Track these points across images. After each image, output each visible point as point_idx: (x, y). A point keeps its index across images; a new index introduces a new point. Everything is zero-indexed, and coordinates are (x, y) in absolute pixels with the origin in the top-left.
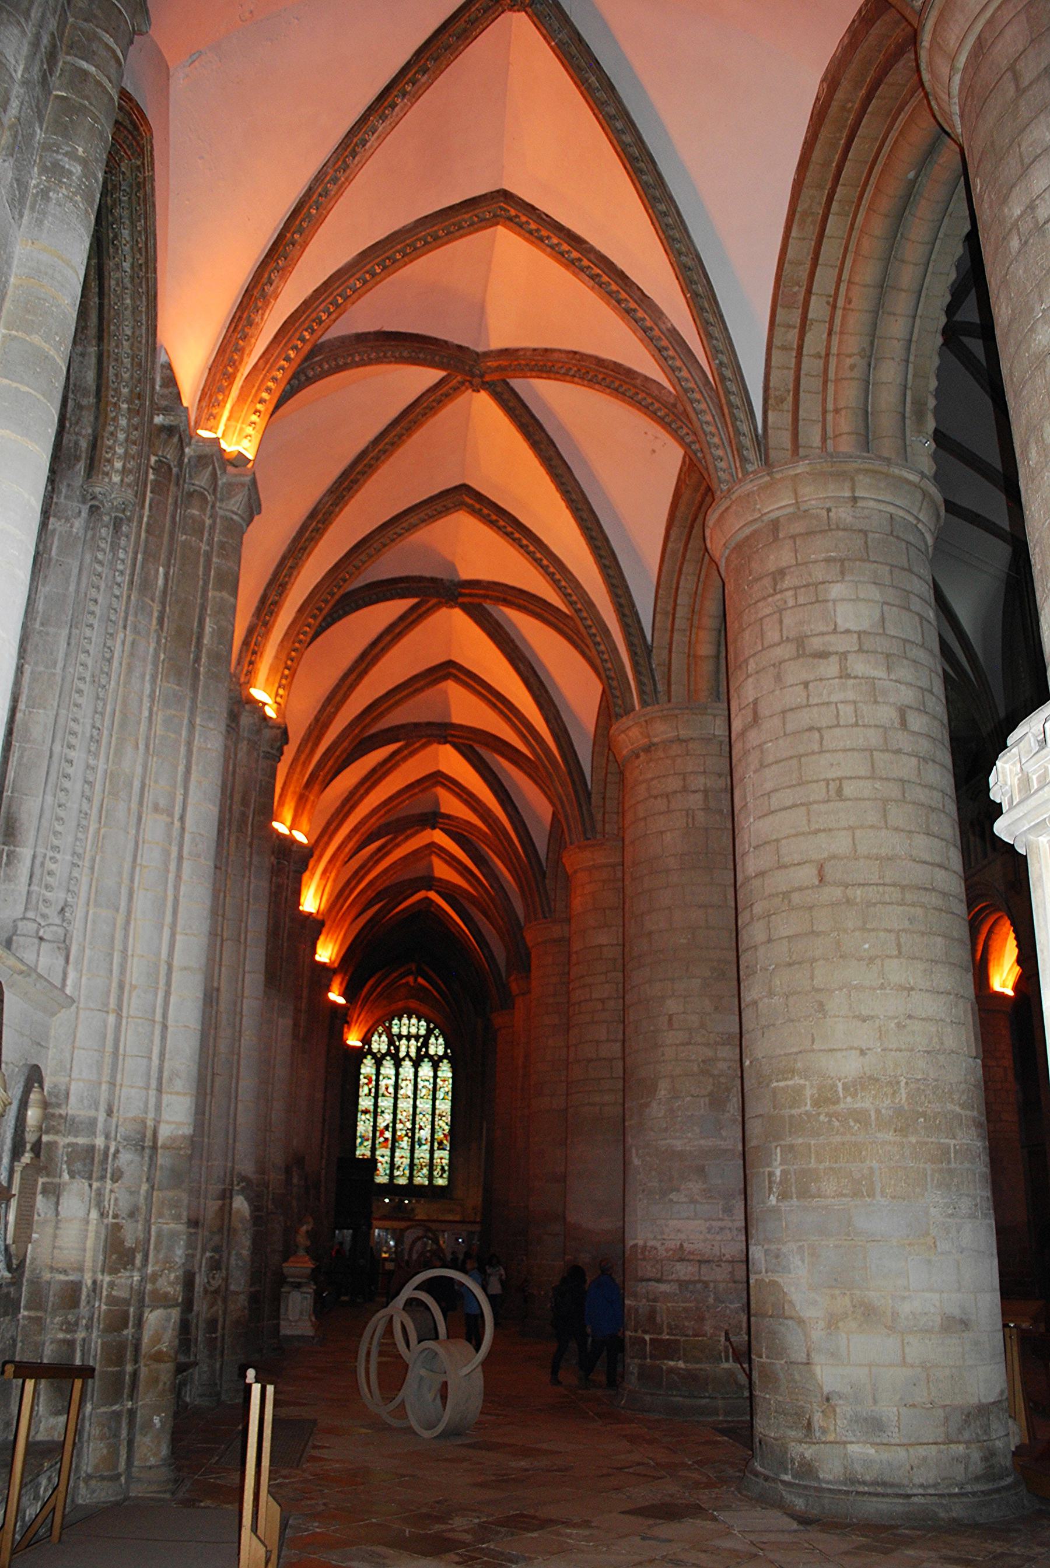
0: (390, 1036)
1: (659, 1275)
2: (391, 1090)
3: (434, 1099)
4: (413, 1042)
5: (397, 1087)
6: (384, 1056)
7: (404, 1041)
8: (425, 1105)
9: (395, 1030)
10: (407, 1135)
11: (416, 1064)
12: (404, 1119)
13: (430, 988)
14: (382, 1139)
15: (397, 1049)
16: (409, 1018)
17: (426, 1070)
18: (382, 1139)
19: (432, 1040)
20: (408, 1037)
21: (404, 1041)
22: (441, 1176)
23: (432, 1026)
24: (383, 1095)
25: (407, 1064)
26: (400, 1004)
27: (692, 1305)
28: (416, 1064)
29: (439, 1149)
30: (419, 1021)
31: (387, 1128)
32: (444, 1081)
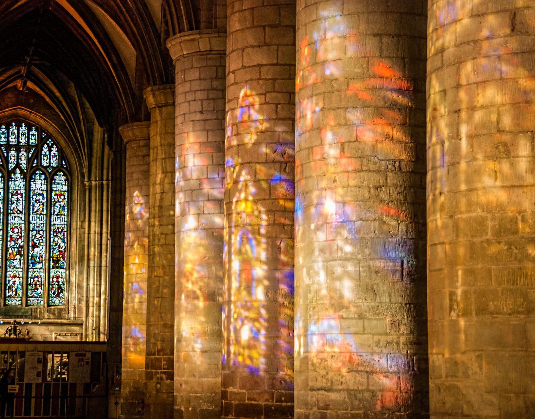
1: (329, 384)
3: (49, 215)
4: (23, 153)
7: (13, 153)
8: (38, 221)
10: (19, 253)
11: (28, 178)
13: (41, 92)
16: (18, 127)
19: (45, 151)
20: (18, 148)
21: (13, 153)
25: (17, 176)
26: (8, 111)
27: (361, 412)
28: (28, 178)
29: (53, 267)
30: (29, 130)
32: (60, 195)
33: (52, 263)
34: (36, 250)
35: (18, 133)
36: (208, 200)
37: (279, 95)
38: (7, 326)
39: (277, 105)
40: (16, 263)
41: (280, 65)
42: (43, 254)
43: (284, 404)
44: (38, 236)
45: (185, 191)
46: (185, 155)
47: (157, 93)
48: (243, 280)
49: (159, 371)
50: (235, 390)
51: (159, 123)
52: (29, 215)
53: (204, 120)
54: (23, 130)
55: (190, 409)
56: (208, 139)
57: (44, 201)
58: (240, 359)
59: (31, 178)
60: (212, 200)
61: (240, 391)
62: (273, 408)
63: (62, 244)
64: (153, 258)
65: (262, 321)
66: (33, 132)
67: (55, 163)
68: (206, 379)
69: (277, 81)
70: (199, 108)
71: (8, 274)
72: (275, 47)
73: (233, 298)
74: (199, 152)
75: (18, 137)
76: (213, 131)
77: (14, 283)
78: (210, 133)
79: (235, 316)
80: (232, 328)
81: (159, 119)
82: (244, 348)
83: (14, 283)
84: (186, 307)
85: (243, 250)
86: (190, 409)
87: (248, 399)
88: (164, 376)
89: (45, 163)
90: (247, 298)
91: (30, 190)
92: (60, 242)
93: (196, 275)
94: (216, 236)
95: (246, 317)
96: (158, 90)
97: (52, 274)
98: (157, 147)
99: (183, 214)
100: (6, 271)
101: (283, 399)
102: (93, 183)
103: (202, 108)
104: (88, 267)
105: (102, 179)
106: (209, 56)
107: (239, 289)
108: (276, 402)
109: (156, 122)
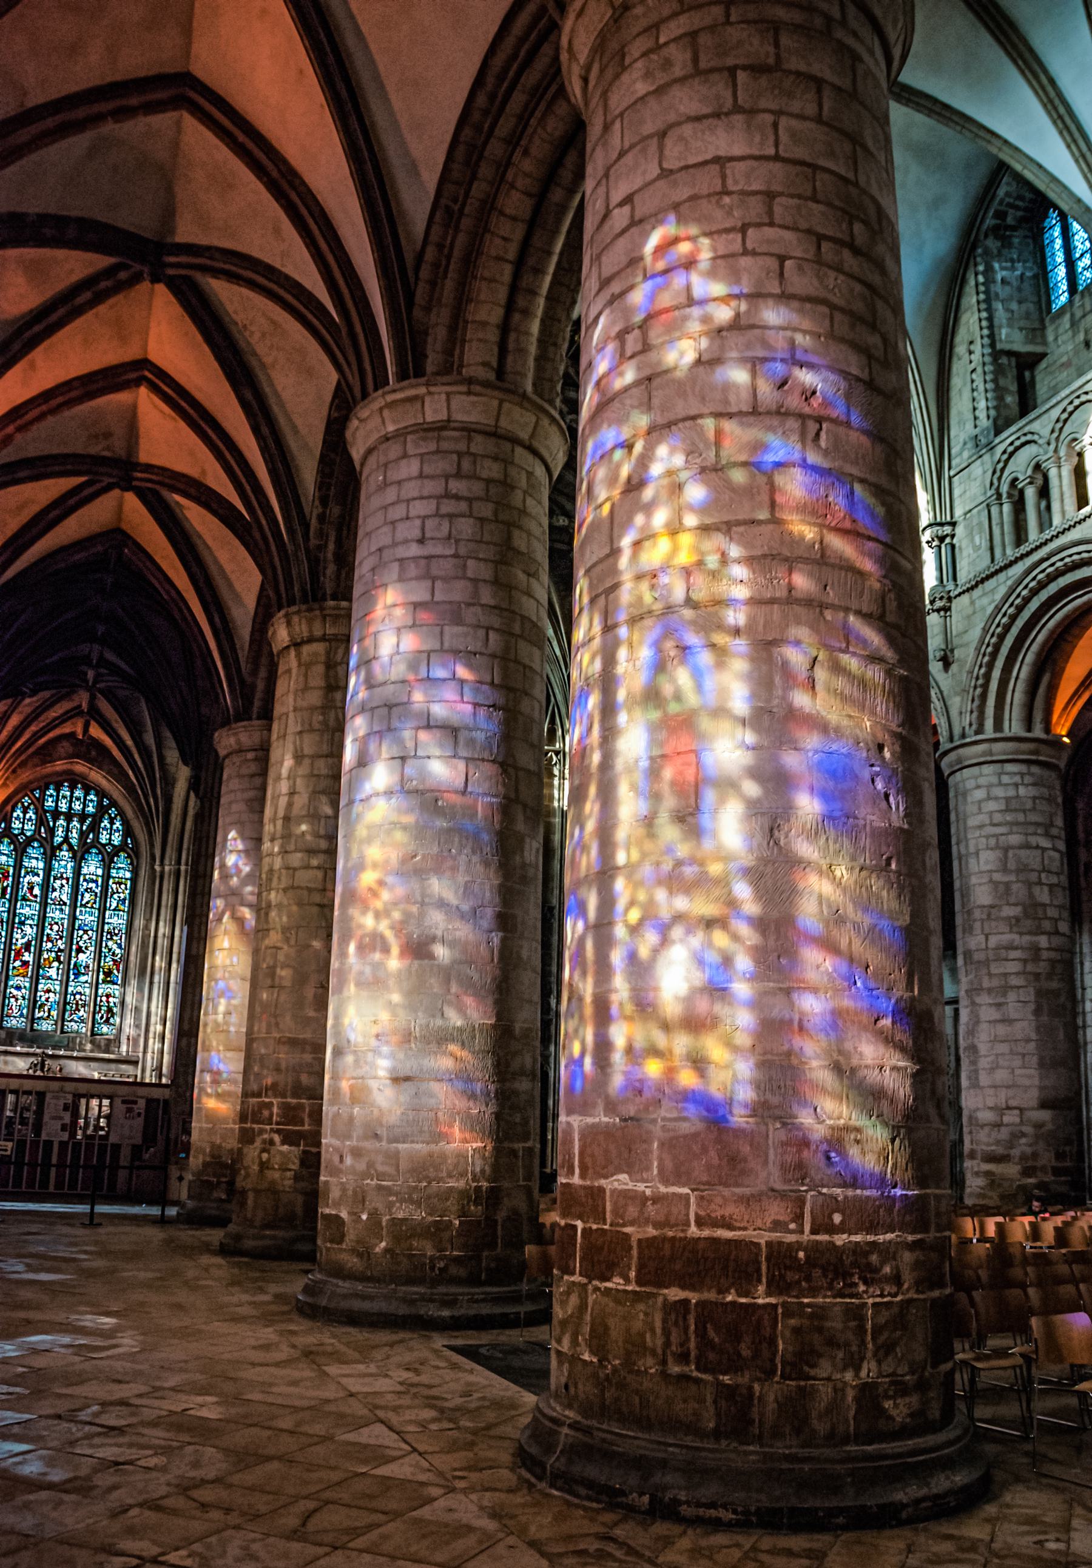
0: (41, 812)
2: (37, 891)
3: (103, 910)
4: (75, 823)
5: (46, 887)
6: (29, 841)
7: (61, 822)
8: (87, 917)
9: (49, 803)
10: (58, 959)
11: (79, 858)
12: (53, 935)
14: (18, 963)
15: (52, 832)
16: (72, 789)
17: (92, 867)
18: (18, 963)
19: (106, 823)
20: (69, 817)
21: (61, 822)
22: (107, 1021)
23: (106, 802)
24: (24, 899)
25: (65, 854)
26: (60, 766)
28: (79, 858)
29: (104, 982)
30: (87, 794)
31: (27, 946)
32: (120, 884)
33: (101, 976)
34: (81, 956)
35: (72, 796)
36: (428, 727)
37: (788, 235)
38: (32, 1059)
39: (782, 259)
40: (52, 972)
41: (785, 160)
42: (90, 962)
43: (840, 1239)
44: (85, 937)
45: (372, 709)
46: (376, 634)
47: (295, 619)
48: (665, 788)
49: (268, 1127)
50: (641, 1187)
51: (294, 671)
52: (75, 907)
53: (426, 558)
54: (78, 793)
55: (364, 1217)
56: (433, 595)
57: (98, 891)
58: (653, 1068)
59: (83, 858)
60: (437, 727)
61: (663, 1189)
62: (801, 1254)
63: (118, 951)
64: (267, 914)
65: (744, 929)
66: (92, 797)
67: (117, 839)
68: (405, 1146)
69: (778, 200)
70: (416, 533)
71: (40, 987)
72: (769, 118)
73: (621, 858)
74: (410, 623)
75: (71, 802)
76: (445, 579)
77: (47, 1000)
78: (439, 584)
79: (634, 916)
80: (617, 957)
81: (294, 664)
82: (666, 1027)
83: (47, 1000)
84: (361, 973)
85: (667, 689)
86: (364, 1217)
87: (700, 1223)
88: (277, 1138)
89: (104, 838)
90: (683, 850)
91: (79, 874)
92: (115, 947)
93: (386, 895)
94: (443, 807)
95: (678, 918)
96: (298, 612)
97: (100, 992)
98: (287, 714)
99: (363, 762)
100: (37, 983)
101: (837, 1218)
102: (167, 868)
103: (423, 533)
104: (151, 983)
105: (179, 863)
106: (445, 433)
107: (649, 822)
108: (814, 1232)
109: (289, 671)
